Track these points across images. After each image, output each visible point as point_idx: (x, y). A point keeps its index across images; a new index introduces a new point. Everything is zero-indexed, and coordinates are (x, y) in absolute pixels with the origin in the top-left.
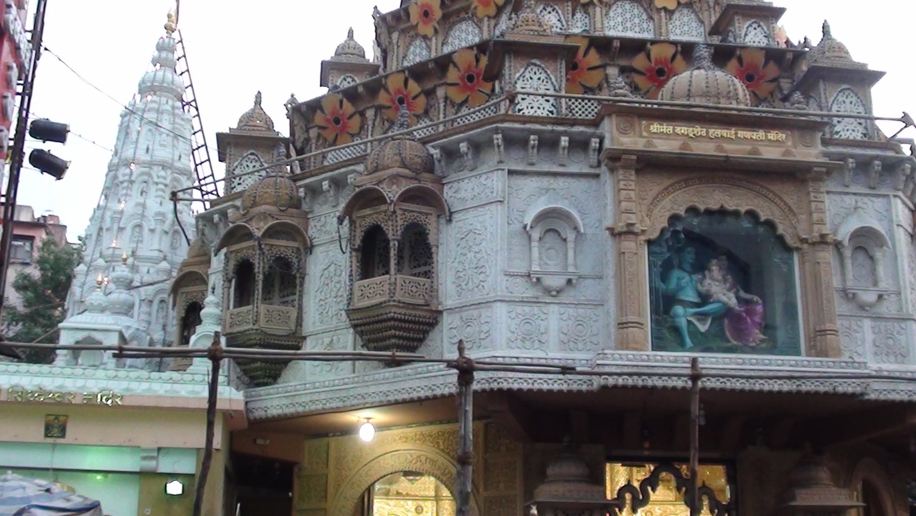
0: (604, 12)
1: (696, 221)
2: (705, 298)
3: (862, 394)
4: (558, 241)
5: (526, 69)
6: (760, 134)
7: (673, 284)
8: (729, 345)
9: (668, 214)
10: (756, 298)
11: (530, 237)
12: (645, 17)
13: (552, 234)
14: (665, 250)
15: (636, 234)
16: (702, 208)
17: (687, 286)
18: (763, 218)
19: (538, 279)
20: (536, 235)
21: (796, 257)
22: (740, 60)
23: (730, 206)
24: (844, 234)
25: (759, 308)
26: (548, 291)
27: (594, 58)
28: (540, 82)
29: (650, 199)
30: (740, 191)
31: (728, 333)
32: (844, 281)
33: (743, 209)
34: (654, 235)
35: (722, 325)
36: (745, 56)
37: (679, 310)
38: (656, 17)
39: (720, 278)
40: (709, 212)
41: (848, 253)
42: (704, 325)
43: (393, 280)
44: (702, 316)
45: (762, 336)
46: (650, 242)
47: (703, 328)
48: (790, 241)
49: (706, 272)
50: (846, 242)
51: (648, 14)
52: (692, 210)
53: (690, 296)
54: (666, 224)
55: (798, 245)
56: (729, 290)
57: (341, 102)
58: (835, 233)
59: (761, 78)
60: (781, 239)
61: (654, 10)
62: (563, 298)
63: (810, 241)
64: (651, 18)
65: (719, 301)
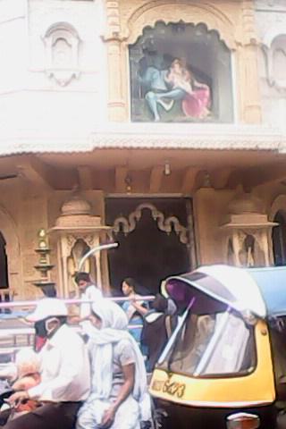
1: (163, 32)
2: (169, 87)
3: (276, 150)
4: (66, 46)
7: (148, 77)
8: (185, 118)
9: (143, 26)
10: (205, 86)
11: (45, 43)
13: (60, 42)
14: (141, 52)
15: (120, 41)
16: (167, 22)
17: (157, 78)
18: (210, 28)
19: (52, 75)
20: (50, 41)
21: (233, 57)
23: (187, 21)
24: (268, 41)
25: (207, 93)
26: (59, 82)
29: (129, 15)
30: (194, 9)
31: (185, 112)
32: (267, 71)
33: (196, 23)
34: (133, 41)
35: (181, 105)
37: (151, 95)
39: (180, 72)
40: (170, 23)
41: (270, 53)
44: (167, 100)
45: (208, 112)
46: (130, 47)
47: (168, 107)
48: (228, 44)
50: (269, 46)
52: (160, 23)
53: (159, 85)
54: (141, 33)
55: (234, 46)
56: (187, 80)
58: (262, 39)
60: (223, 43)
62: (68, 88)
63: (243, 44)
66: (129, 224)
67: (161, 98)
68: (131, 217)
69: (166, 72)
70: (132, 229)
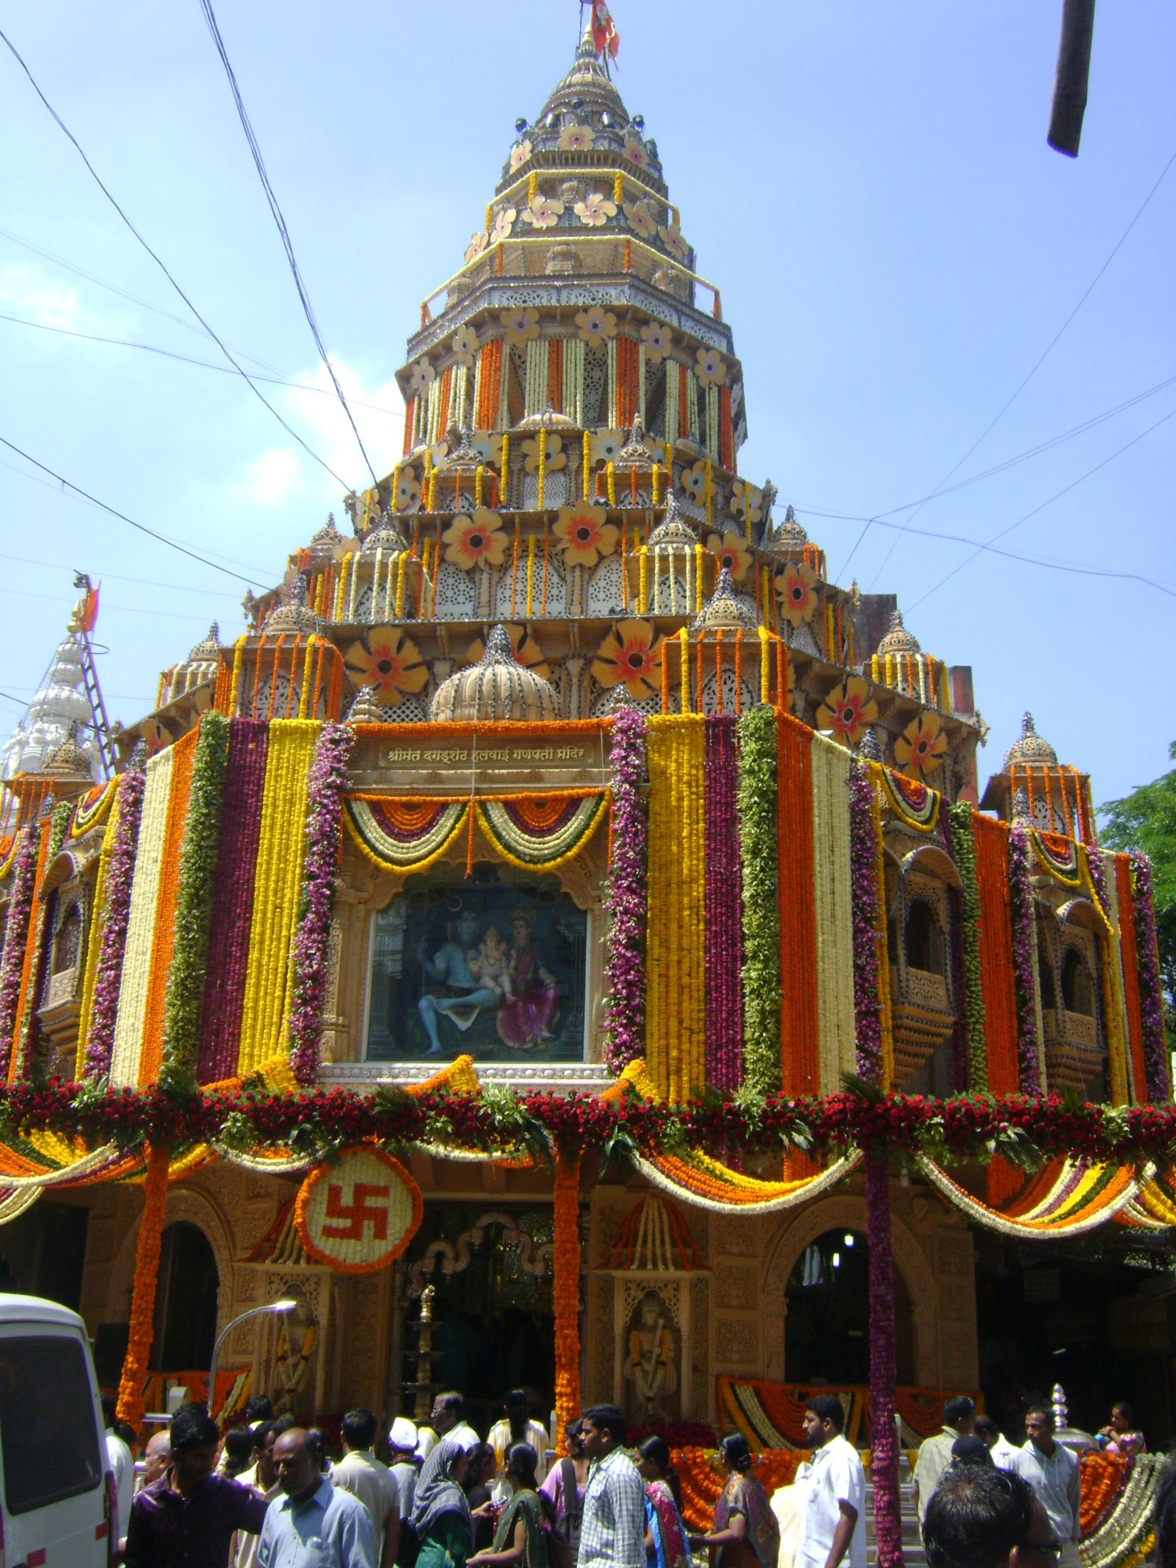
0: (495, 578)
5: (265, 683)
6: (548, 753)
12: (556, 579)
22: (619, 639)
27: (411, 653)
28: (283, 699)
31: (501, 1032)
36: (626, 631)
38: (569, 578)
42: (467, 1019)
43: (77, 973)
45: (546, 1034)
47: (463, 1025)
49: (482, 947)
51: (559, 576)
57: (158, 728)
59: (650, 660)
61: (568, 570)
64: (563, 579)
65: (486, 988)
66: (457, 1258)
67: (451, 1008)
68: (464, 1237)
69: (471, 953)
70: (461, 1266)
